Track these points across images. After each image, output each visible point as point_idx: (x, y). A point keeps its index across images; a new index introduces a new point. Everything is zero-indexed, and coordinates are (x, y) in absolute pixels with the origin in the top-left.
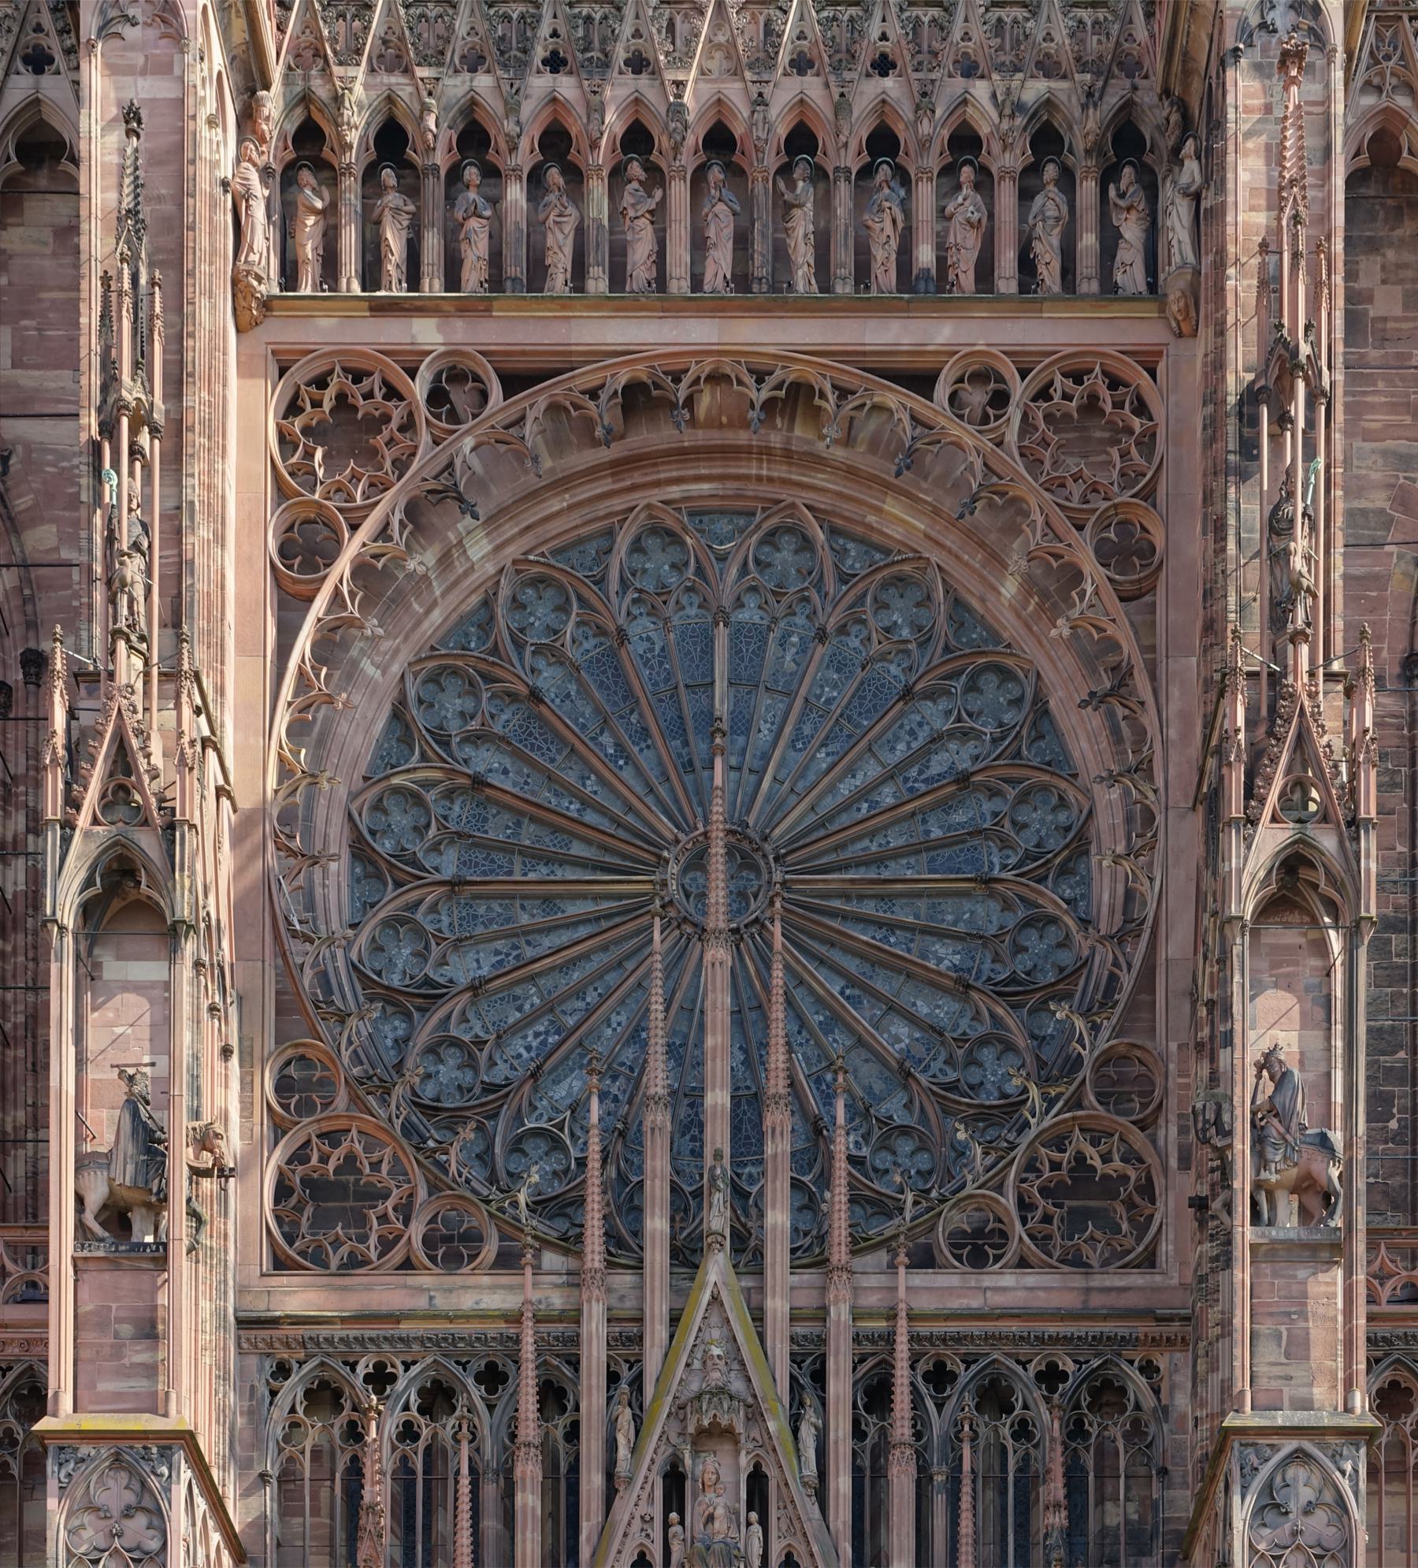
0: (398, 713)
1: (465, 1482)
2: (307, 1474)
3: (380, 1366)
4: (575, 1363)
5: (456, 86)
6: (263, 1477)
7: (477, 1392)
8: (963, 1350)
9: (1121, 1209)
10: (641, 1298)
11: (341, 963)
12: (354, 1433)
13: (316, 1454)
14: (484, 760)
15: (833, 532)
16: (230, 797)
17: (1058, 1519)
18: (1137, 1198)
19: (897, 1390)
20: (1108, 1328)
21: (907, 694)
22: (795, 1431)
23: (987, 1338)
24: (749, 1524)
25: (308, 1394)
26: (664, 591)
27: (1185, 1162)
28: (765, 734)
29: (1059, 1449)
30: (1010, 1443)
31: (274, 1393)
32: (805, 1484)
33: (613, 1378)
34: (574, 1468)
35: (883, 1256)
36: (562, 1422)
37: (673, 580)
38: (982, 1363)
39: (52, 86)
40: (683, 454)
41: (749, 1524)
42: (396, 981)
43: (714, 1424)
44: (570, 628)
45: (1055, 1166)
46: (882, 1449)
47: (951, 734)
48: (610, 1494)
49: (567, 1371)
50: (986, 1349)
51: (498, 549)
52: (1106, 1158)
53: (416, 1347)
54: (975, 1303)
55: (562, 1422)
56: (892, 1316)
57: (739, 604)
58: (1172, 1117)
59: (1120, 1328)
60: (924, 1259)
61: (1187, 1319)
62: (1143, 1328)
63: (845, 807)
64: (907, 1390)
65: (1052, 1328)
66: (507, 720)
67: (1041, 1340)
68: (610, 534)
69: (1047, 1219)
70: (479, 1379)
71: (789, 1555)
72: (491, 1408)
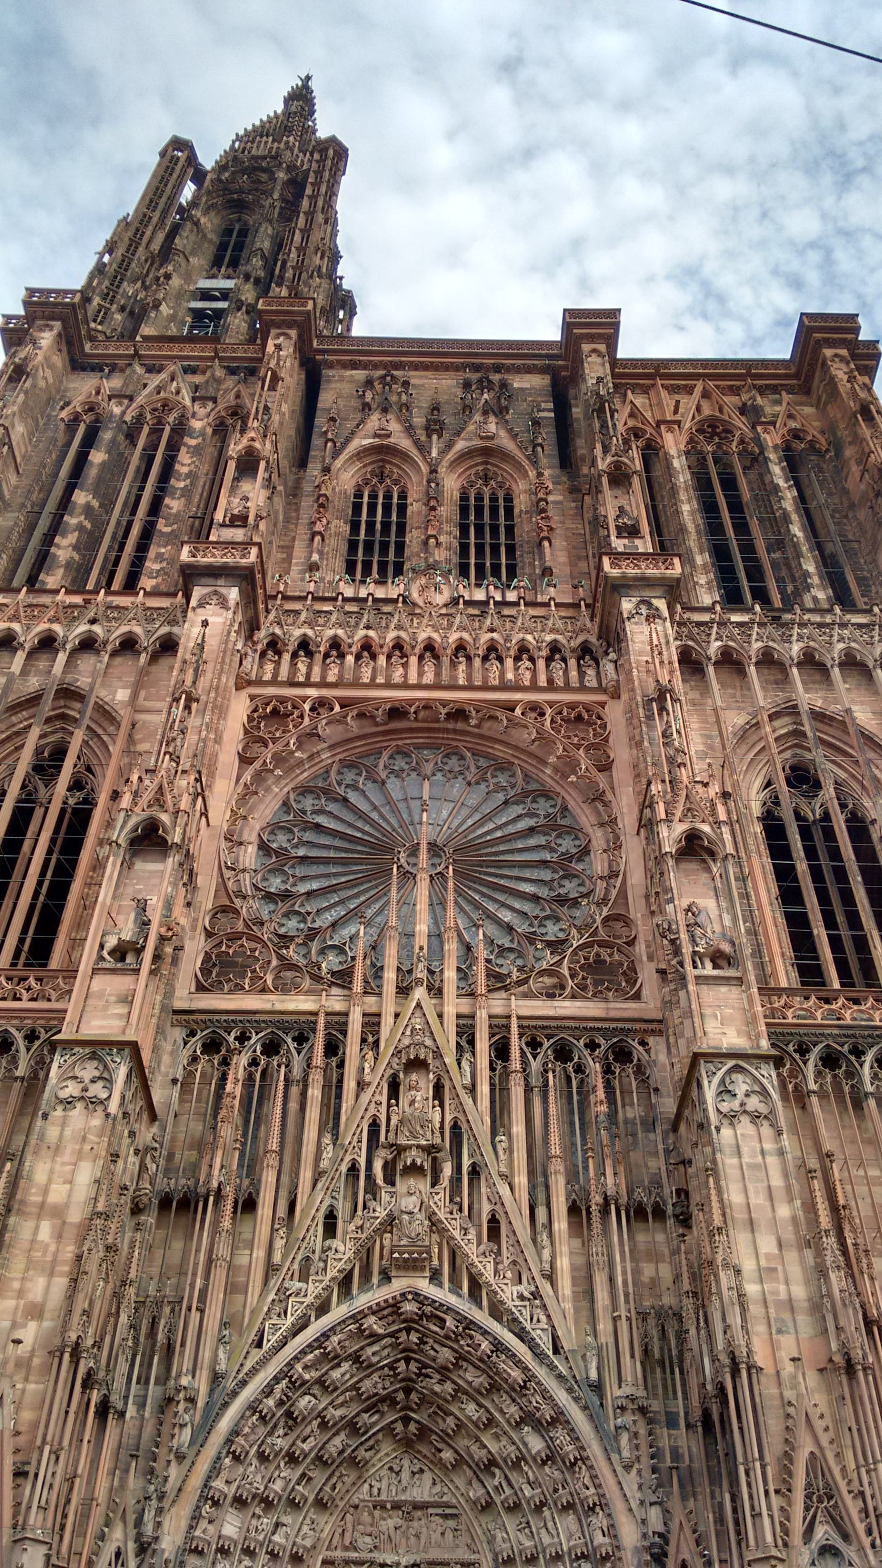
0: (286, 804)
1: (281, 1084)
2: (197, 1081)
3: (243, 1034)
4: (344, 1033)
5: (330, 633)
6: (174, 1081)
7: (292, 1045)
8: (546, 1032)
9: (622, 978)
10: (381, 1006)
11: (248, 882)
12: (225, 1062)
13: (203, 1075)
14: (321, 820)
15: (473, 754)
16: (207, 817)
17: (604, 1108)
18: (628, 972)
19: (513, 1051)
20: (620, 1025)
21: (506, 802)
22: (459, 1064)
23: (557, 1028)
24: (434, 1107)
25: (204, 1045)
26: (403, 771)
27: (650, 958)
28: (445, 814)
29: (600, 1076)
30: (573, 1075)
31: (186, 1044)
32: (465, 1088)
33: (364, 1040)
34: (340, 1080)
35: (503, 994)
36: (334, 1061)
37: (406, 767)
38: (556, 1039)
39: (176, 630)
40: (411, 730)
41: (434, 1107)
42: (272, 890)
43: (417, 1057)
44: (361, 780)
45: (586, 959)
46: (506, 1074)
47: (526, 815)
48: (361, 1085)
49: (340, 1037)
50: (557, 1032)
51: (333, 756)
52: (610, 955)
53: (263, 1025)
54: (551, 1013)
55: (334, 1061)
56: (509, 1017)
57: (434, 774)
58: (642, 941)
59: (628, 1026)
60: (526, 996)
61: (660, 1021)
62: (637, 1026)
63: (480, 836)
64: (518, 1052)
65: (591, 1025)
66: (332, 807)
67: (585, 1028)
68: (381, 753)
69: (584, 978)
70: (294, 1039)
71: (456, 1123)
72: (299, 1053)
